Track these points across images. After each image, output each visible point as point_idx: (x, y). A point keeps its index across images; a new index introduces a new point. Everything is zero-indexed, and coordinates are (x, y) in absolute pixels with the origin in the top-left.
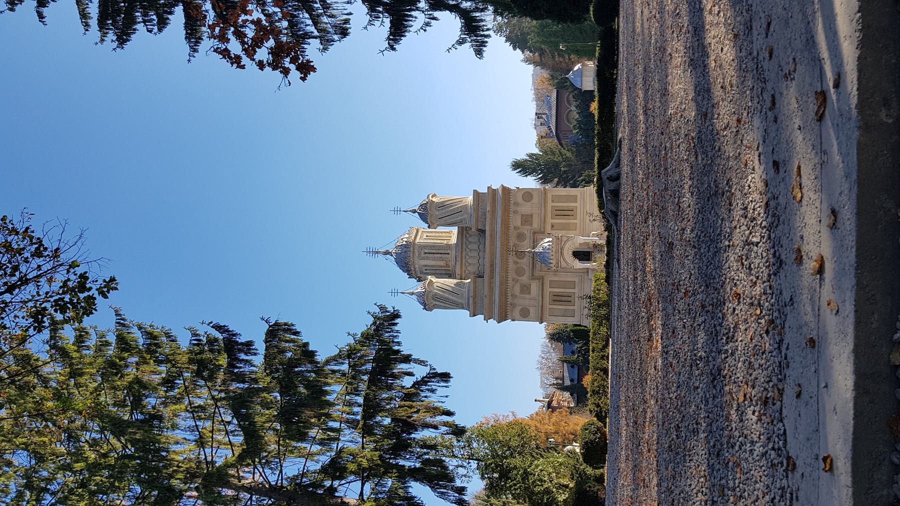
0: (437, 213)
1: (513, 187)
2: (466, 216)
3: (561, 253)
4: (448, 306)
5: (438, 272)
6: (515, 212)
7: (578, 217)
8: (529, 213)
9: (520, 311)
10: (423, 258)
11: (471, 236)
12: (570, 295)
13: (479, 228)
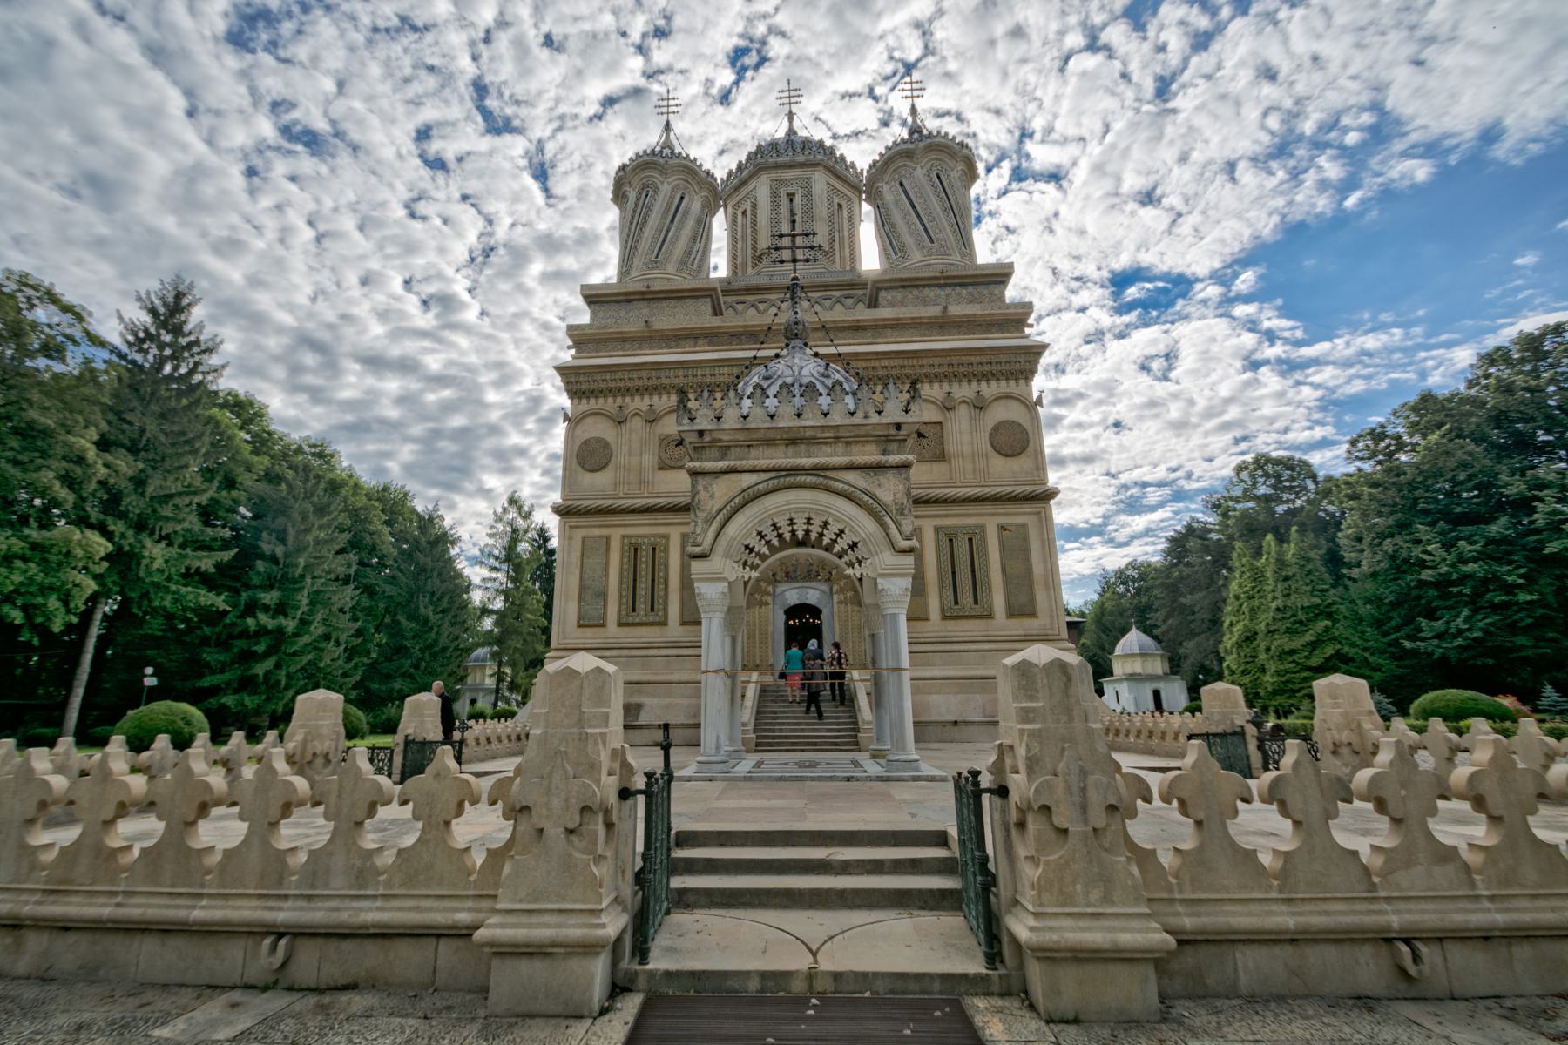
8: (951, 446)
9: (598, 440)
10: (775, 195)
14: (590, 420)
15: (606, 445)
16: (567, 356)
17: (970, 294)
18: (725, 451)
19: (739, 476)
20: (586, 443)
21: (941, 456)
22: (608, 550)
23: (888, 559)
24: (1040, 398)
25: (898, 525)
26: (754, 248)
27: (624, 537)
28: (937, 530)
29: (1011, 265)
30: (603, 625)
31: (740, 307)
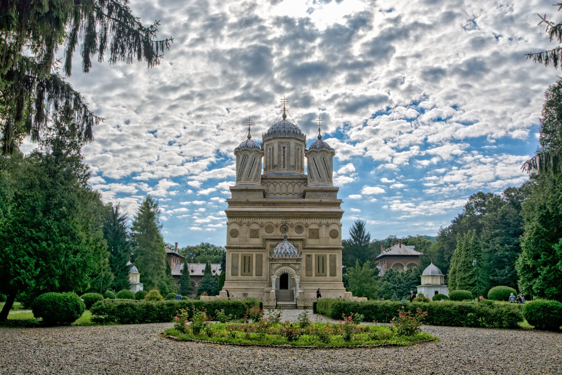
8: (320, 235)
9: (235, 230)
10: (279, 147)
11: (300, 186)
14: (233, 224)
15: (237, 231)
18: (276, 260)
20: (232, 230)
21: (318, 237)
23: (296, 276)
26: (273, 162)
28: (316, 255)
29: (338, 188)
31: (269, 184)
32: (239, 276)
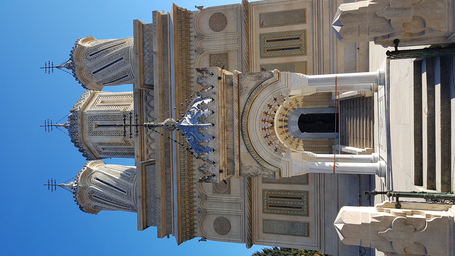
0: (89, 64)
1: (191, 8)
2: (128, 66)
3: (240, 128)
4: (114, 208)
5: (119, 151)
6: (199, 51)
7: (309, 50)
8: (221, 50)
9: (215, 223)
10: (95, 134)
12: (299, 195)
13: (147, 82)
15: (217, 219)
16: (173, 239)
17: (148, 40)
19: (241, 153)
22: (270, 220)
24: (199, 8)
25: (266, 79)
27: (264, 212)
30: (308, 224)
31: (150, 152)
32: (310, 219)
